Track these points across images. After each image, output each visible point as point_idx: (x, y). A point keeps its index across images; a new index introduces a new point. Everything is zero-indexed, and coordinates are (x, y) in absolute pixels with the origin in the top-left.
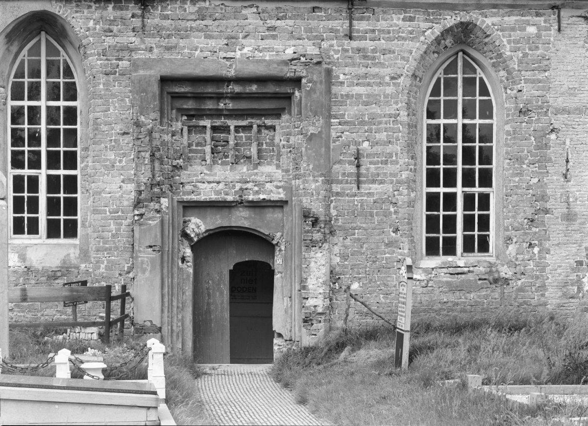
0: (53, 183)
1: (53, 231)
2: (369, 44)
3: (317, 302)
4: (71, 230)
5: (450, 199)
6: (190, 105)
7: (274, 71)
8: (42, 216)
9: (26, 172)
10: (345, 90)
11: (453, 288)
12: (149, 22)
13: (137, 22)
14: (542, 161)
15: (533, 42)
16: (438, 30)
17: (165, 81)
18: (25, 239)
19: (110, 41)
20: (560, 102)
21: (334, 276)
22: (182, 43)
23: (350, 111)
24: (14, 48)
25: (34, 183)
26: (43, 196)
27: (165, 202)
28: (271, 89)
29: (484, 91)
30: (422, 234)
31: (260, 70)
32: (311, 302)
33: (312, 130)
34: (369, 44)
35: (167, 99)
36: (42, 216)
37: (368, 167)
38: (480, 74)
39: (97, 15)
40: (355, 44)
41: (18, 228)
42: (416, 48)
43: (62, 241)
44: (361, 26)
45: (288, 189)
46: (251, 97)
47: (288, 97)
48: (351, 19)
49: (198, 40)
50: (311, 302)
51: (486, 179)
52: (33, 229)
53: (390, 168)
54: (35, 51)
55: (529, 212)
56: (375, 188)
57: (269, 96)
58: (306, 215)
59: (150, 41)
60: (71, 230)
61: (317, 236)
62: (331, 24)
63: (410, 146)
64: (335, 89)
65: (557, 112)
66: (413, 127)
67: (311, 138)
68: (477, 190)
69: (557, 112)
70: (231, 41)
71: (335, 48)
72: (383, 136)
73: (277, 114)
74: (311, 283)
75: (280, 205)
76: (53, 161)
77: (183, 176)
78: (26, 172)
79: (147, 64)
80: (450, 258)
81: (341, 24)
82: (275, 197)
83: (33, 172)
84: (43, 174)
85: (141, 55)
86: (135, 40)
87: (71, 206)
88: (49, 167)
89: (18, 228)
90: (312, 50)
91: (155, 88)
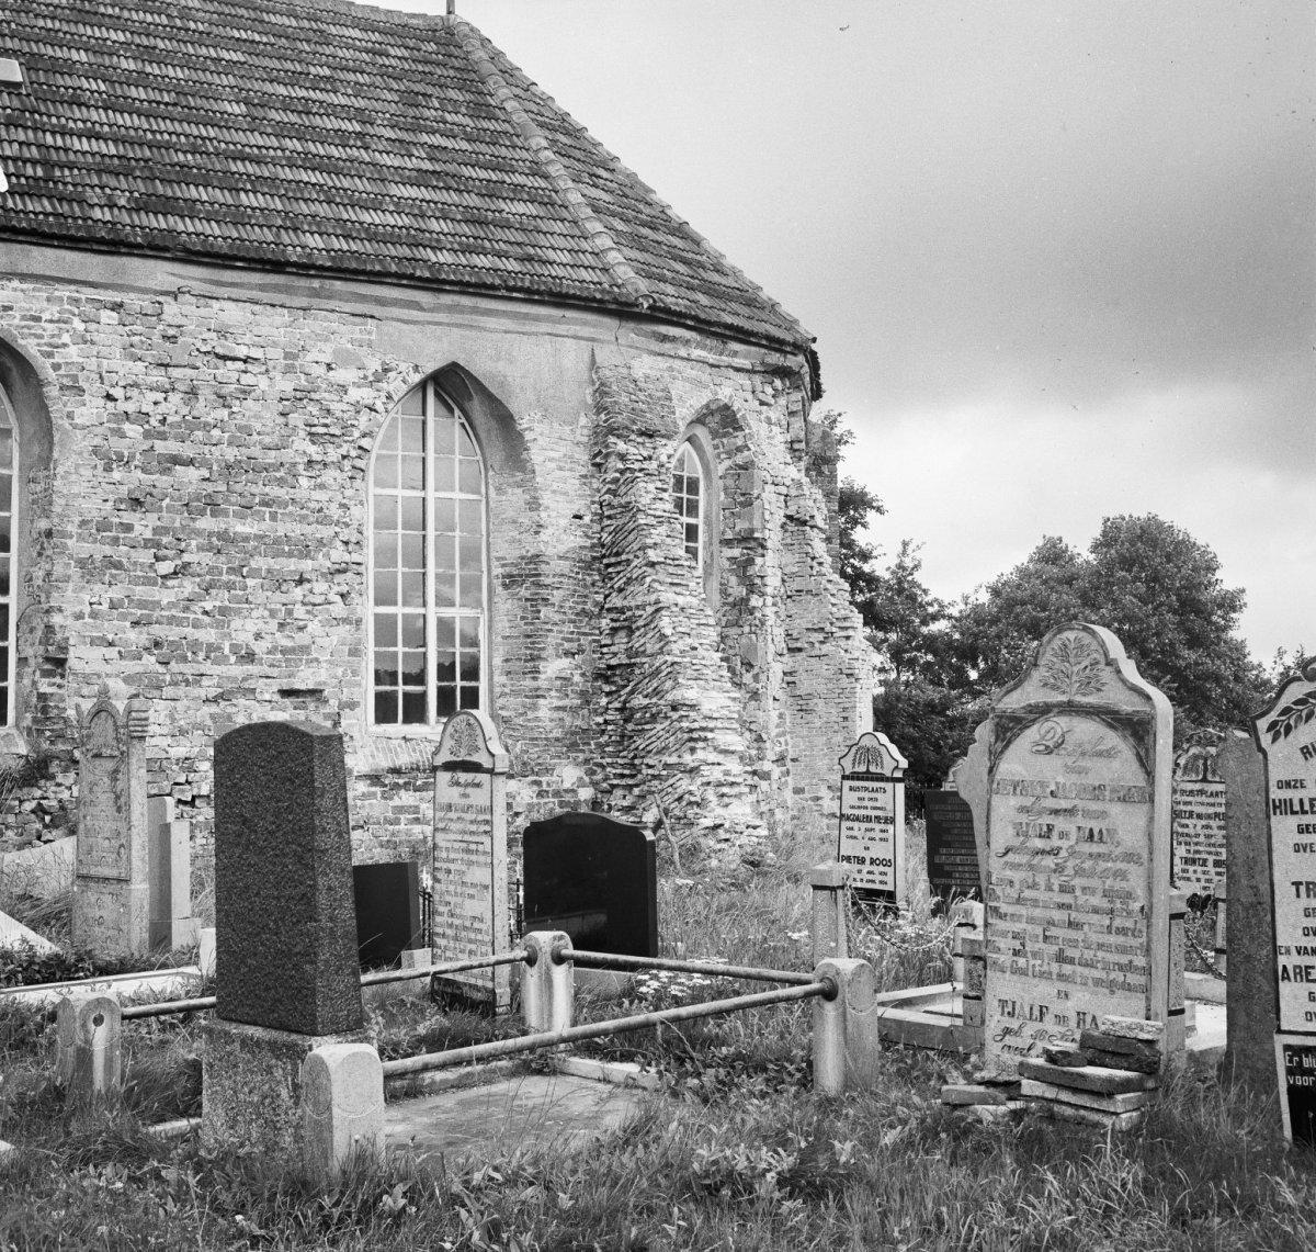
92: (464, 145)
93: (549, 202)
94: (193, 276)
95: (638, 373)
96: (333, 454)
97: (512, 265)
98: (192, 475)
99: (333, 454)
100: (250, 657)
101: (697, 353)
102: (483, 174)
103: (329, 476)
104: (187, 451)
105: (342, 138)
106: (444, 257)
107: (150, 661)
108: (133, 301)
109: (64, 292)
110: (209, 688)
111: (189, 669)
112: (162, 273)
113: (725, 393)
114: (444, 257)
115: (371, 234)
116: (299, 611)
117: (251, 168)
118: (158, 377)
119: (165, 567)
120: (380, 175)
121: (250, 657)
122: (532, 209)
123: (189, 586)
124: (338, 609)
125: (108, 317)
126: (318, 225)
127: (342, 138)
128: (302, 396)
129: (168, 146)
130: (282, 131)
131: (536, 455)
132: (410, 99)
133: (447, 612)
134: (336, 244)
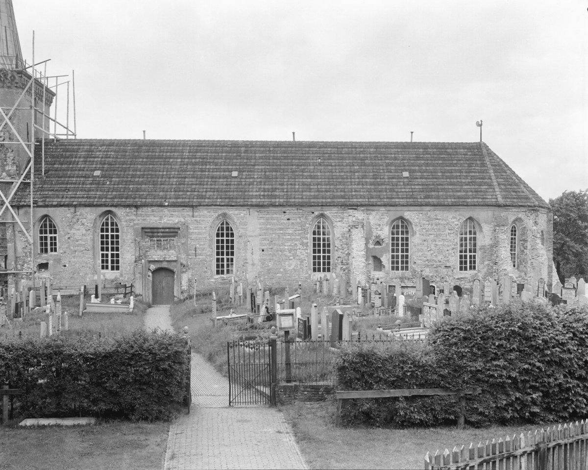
0: (112, 255)
1: (113, 268)
2: (198, 219)
3: (185, 287)
4: (118, 268)
5: (223, 259)
6: (150, 234)
7: (172, 226)
8: (110, 264)
9: (105, 252)
10: (192, 231)
11: (222, 284)
12: (138, 213)
13: (135, 213)
14: (246, 250)
15: (243, 218)
16: (217, 215)
17: (142, 228)
18: (105, 271)
19: (128, 218)
20: (250, 234)
21: (190, 281)
22: (147, 218)
23: (194, 237)
24: (101, 219)
25: (107, 255)
26: (110, 259)
27: (143, 261)
28: (172, 230)
29: (232, 230)
30: (215, 269)
31: (169, 226)
32: (183, 288)
33: (183, 242)
34: (198, 219)
35: (144, 233)
36: (110, 264)
37: (198, 251)
38: (230, 226)
39: (124, 211)
40: (195, 219)
41: (103, 268)
42: (211, 220)
43: (115, 271)
44: (196, 214)
45: (177, 257)
46: (167, 232)
47: (177, 232)
48: (193, 212)
49: (152, 218)
50: (183, 288)
51: (232, 254)
52: (107, 268)
53: (205, 252)
54: (107, 219)
55: (242, 263)
56: (201, 257)
57: (172, 232)
58: (182, 264)
59: (139, 218)
60: (118, 268)
61: (184, 270)
62: (188, 213)
63: (210, 246)
64: (189, 231)
65: (250, 236)
66: (211, 240)
67: (183, 244)
68: (230, 257)
69: (250, 236)
70: (161, 218)
71: (189, 219)
72: (202, 243)
73: (174, 236)
74: (183, 283)
75: (175, 261)
76: (113, 249)
77: (149, 253)
78: (105, 252)
79: (138, 224)
80: (222, 276)
81: (191, 213)
82: (174, 259)
83: (107, 252)
84: (110, 253)
85: (136, 222)
86: (134, 217)
87: (118, 262)
88: (111, 251)
89: (103, 268)
90: (183, 220)
91: (140, 231)
92: (478, 174)
93: (490, 185)
94: (432, 208)
95: (502, 215)
96: (452, 232)
97: (480, 200)
98: (433, 236)
99: (452, 232)
100: (440, 262)
101: (514, 210)
102: (480, 180)
103: (452, 235)
104: (431, 233)
105: (456, 177)
106: (469, 200)
107: (427, 262)
108: (424, 212)
109: (415, 212)
110: (435, 266)
111: (432, 263)
112: (428, 208)
113: (520, 216)
114: (469, 200)
115: (459, 198)
116: (447, 255)
117: (441, 187)
118: (427, 223)
119: (429, 249)
120: (462, 184)
121: (440, 262)
122: (487, 187)
123: (432, 252)
124: (453, 255)
125: (421, 215)
126: (450, 197)
127: (456, 177)
128: (448, 224)
129: (429, 185)
130: (447, 177)
131: (484, 230)
132: (470, 166)
133: (471, 254)
134: (453, 200)
